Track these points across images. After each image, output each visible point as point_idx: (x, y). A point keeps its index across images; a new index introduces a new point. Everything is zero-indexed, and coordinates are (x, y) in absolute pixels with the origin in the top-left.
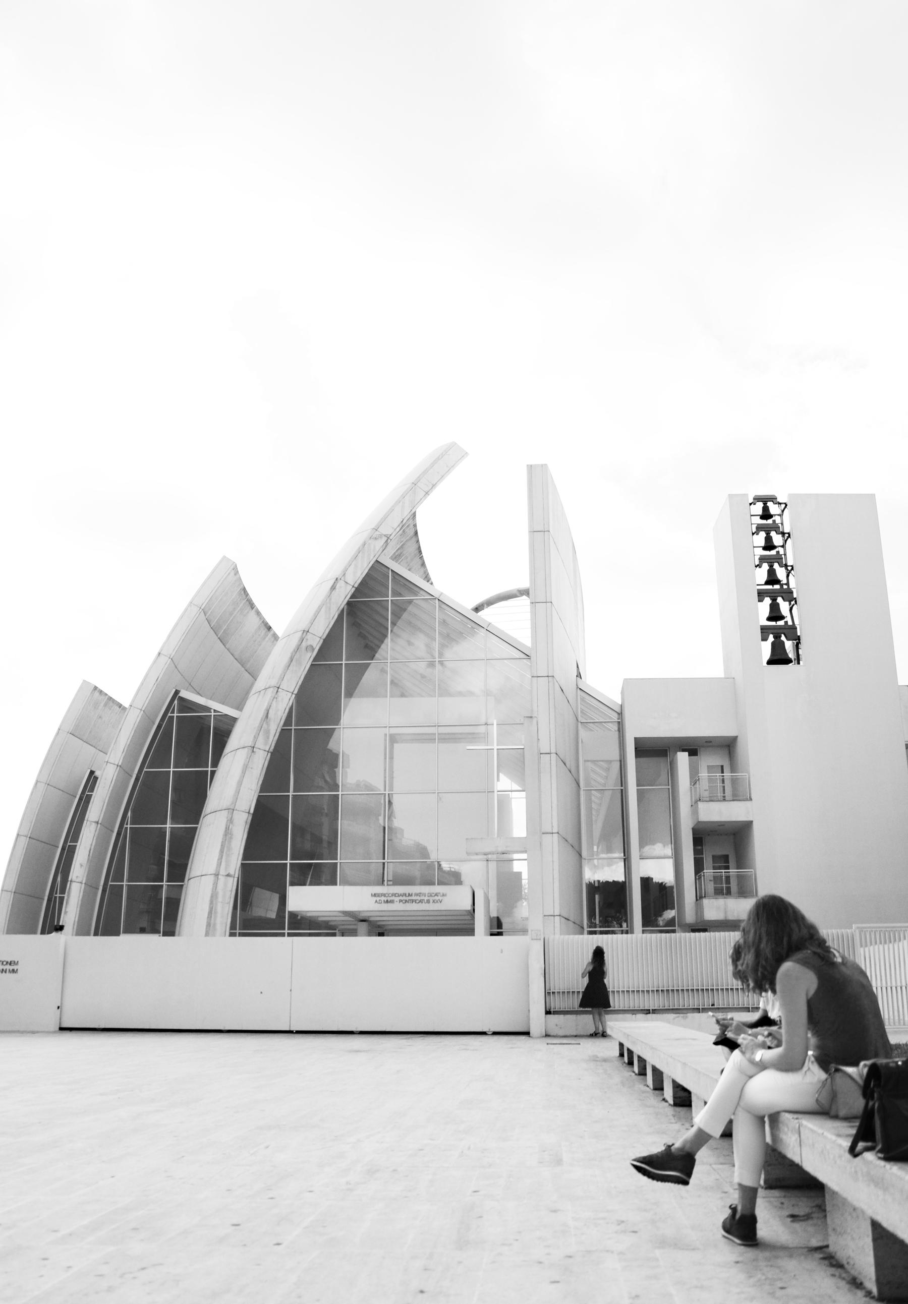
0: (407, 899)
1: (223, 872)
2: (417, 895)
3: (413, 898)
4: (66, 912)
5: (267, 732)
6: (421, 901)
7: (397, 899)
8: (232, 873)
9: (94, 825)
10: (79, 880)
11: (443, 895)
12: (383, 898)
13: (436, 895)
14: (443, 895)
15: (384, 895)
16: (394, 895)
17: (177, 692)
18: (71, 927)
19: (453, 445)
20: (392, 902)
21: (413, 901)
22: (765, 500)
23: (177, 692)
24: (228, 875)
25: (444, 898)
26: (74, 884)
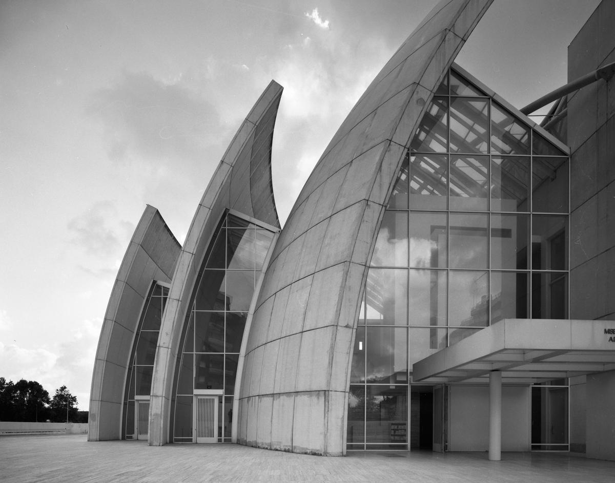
1: (342, 323)
4: (156, 371)
5: (381, 186)
8: (351, 324)
18: (162, 382)
24: (347, 326)
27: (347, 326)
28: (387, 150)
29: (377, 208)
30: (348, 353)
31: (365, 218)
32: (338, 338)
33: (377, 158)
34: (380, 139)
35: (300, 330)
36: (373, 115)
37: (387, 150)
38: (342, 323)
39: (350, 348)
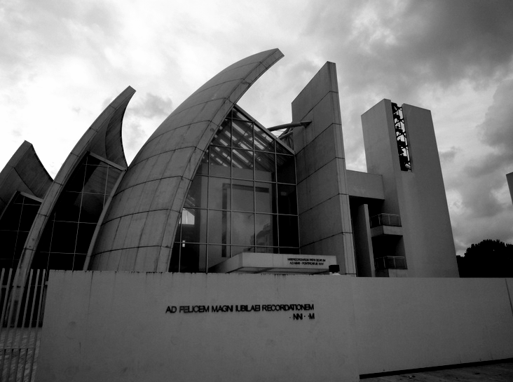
0: (306, 262)
2: (311, 260)
3: (309, 261)
5: (190, 170)
6: (313, 264)
7: (301, 262)
8: (169, 245)
9: (43, 217)
10: (32, 248)
11: (324, 260)
12: (294, 261)
13: (321, 260)
14: (324, 260)
15: (295, 259)
16: (299, 259)
17: (88, 153)
19: (277, 50)
20: (299, 263)
21: (309, 263)
22: (394, 105)
23: (88, 153)
24: (167, 247)
25: (325, 263)
26: (27, 251)
27: (167, 247)
28: (194, 152)
29: (188, 181)
30: (167, 263)
31: (180, 186)
32: (161, 253)
33: (188, 155)
34: (190, 145)
35: (137, 246)
36: (186, 127)
37: (194, 152)
38: (164, 244)
39: (168, 260)
